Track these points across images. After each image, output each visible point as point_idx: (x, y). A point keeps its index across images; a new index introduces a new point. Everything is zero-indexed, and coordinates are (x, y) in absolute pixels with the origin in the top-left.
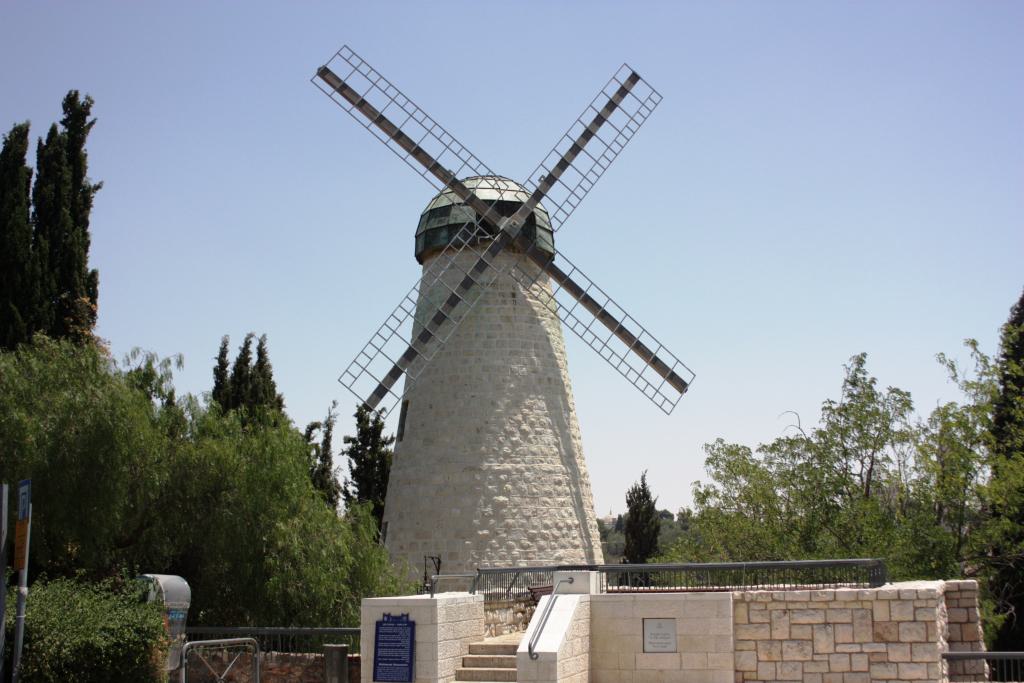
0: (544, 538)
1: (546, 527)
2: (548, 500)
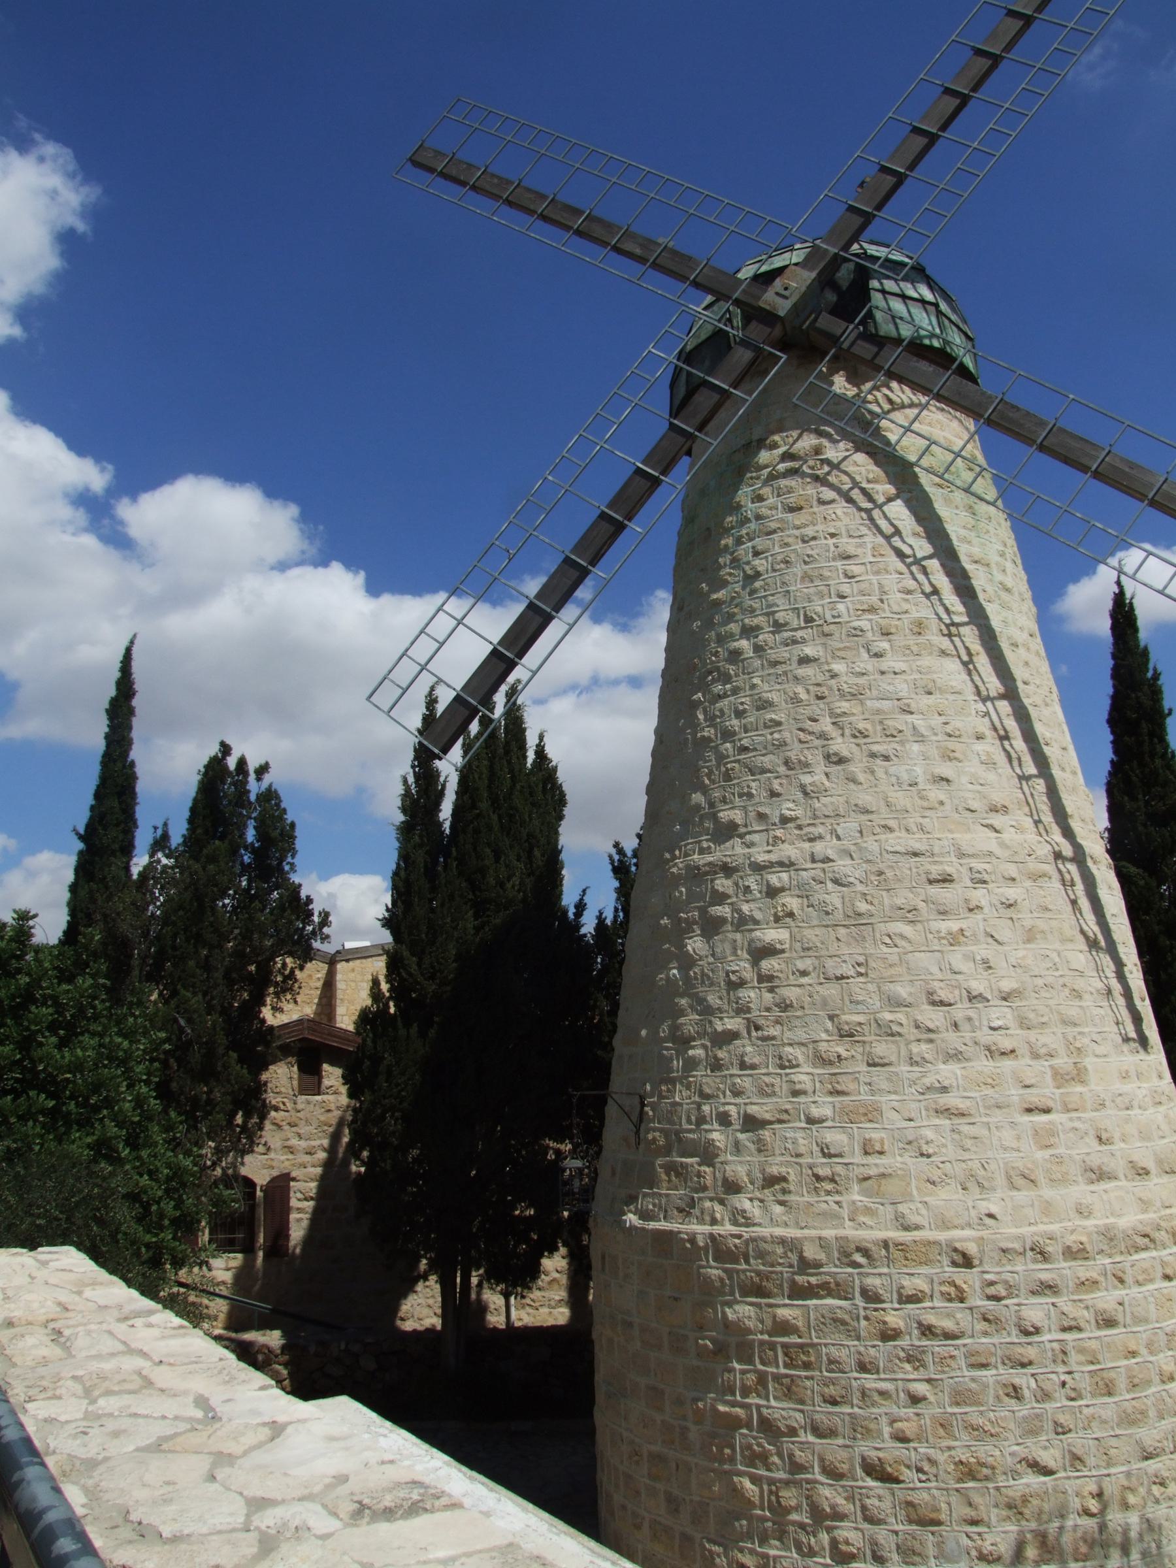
0: (890, 1033)
1: (896, 1003)
2: (907, 930)
